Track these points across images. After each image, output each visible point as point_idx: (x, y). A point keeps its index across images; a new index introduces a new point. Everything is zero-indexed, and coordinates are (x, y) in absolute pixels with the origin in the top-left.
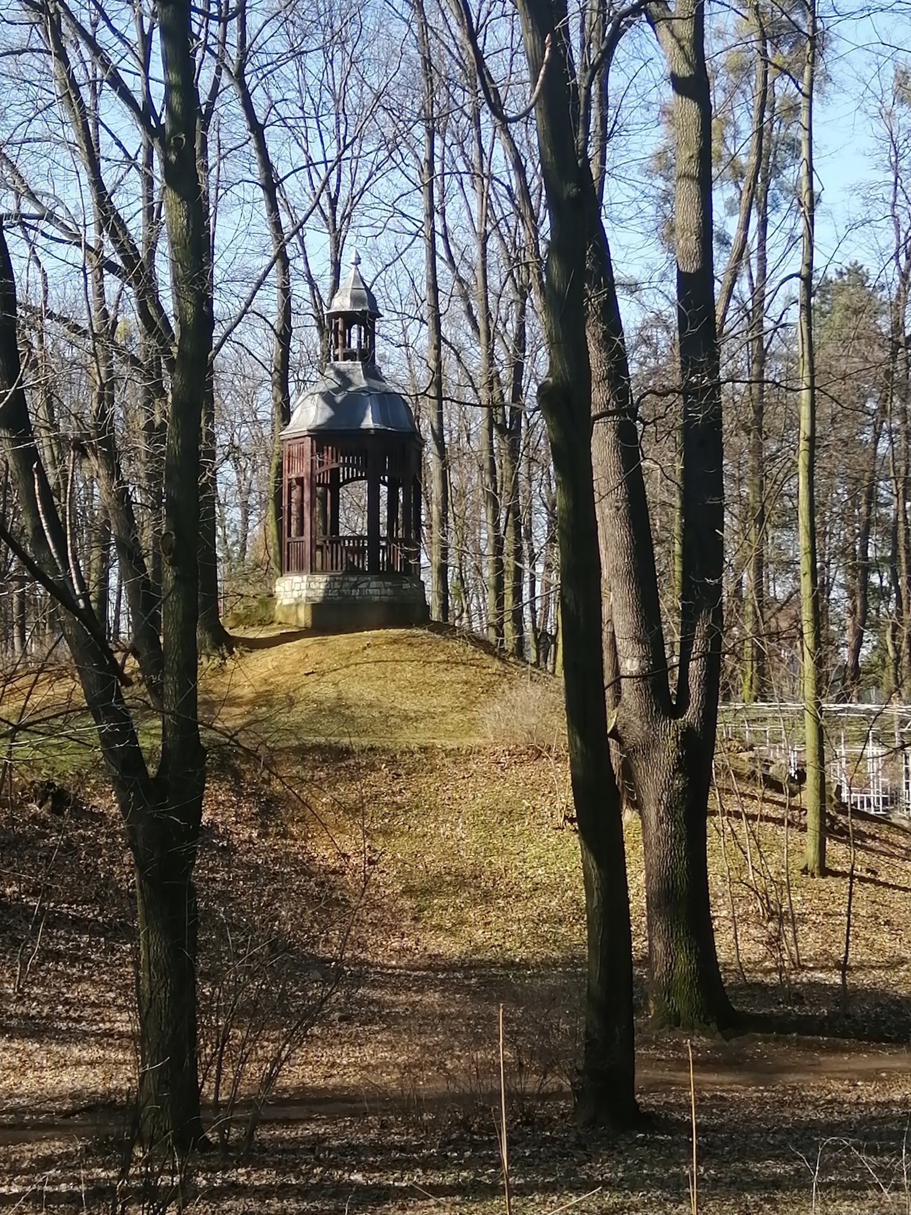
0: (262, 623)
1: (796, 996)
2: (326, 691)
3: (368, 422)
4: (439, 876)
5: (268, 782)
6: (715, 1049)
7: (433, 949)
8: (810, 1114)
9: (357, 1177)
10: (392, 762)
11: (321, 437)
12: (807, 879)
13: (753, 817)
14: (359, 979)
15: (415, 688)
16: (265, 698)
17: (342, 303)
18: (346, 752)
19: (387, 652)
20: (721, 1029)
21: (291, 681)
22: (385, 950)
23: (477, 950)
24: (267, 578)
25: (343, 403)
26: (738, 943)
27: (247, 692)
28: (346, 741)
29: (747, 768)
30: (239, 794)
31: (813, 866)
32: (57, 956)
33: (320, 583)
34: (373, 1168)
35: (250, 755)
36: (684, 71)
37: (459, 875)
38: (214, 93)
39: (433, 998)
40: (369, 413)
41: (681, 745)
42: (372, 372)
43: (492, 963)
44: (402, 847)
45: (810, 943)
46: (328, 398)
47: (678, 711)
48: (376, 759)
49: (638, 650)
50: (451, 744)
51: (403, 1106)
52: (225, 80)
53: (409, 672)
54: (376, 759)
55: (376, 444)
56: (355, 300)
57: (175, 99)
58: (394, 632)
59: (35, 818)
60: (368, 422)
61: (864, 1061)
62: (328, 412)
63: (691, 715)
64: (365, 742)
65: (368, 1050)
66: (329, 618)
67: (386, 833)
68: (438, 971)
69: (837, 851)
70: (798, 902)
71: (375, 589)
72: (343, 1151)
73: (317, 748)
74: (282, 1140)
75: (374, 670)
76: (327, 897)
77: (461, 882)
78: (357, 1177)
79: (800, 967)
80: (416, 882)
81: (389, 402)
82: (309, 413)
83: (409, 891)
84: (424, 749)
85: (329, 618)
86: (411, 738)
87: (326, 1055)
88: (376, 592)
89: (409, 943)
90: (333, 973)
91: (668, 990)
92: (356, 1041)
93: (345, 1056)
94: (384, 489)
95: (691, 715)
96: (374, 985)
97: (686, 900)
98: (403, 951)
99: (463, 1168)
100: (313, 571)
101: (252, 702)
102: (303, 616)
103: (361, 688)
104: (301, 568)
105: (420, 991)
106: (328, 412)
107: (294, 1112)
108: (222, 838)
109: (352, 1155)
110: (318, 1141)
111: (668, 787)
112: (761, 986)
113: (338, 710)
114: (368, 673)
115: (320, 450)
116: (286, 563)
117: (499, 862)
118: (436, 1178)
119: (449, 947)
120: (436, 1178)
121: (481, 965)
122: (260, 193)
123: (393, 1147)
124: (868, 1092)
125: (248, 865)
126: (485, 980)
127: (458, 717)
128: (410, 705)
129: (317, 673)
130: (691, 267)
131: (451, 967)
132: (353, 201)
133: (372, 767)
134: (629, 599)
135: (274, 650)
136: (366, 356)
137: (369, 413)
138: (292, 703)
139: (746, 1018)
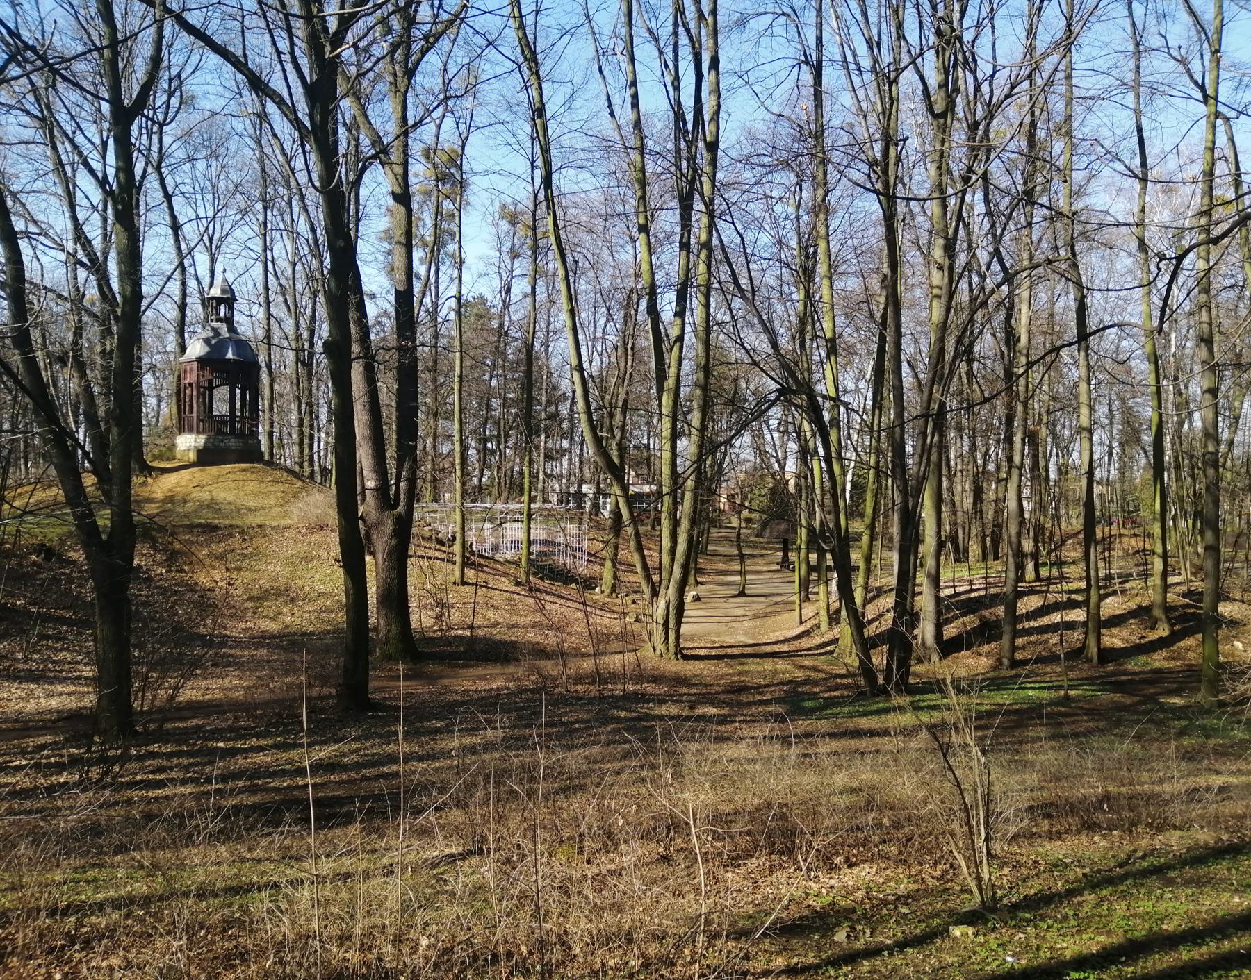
0: (168, 459)
1: (449, 641)
2: (205, 495)
3: (230, 355)
4: (267, 591)
5: (171, 543)
6: (409, 670)
7: (263, 627)
8: (455, 698)
9: (221, 744)
10: (242, 533)
11: (201, 360)
12: (455, 587)
13: (430, 558)
14: (223, 644)
15: (256, 494)
16: (170, 499)
17: (216, 292)
18: (216, 528)
19: (240, 476)
22: (235, 629)
23: (287, 627)
25: (216, 346)
26: (421, 619)
27: (159, 496)
29: (428, 535)
30: (155, 550)
31: (458, 581)
32: (48, 637)
33: (202, 439)
34: (229, 739)
35: (162, 529)
36: (398, 191)
37: (278, 589)
38: (144, 176)
42: (232, 329)
43: (295, 634)
44: (247, 576)
45: (456, 617)
46: (207, 341)
47: (395, 506)
50: (275, 523)
53: (252, 486)
55: (233, 366)
56: (223, 291)
57: (121, 176)
59: (34, 564)
60: (230, 355)
61: (480, 671)
62: (207, 349)
63: (401, 508)
64: (227, 522)
65: (227, 680)
66: (206, 457)
67: (239, 569)
68: (265, 639)
69: (470, 573)
70: (451, 597)
71: (232, 443)
72: (212, 732)
73: (200, 525)
74: (179, 728)
75: (232, 485)
76: (205, 603)
77: (279, 593)
78: (221, 744)
79: (450, 628)
80: (254, 594)
81: (241, 345)
82: (196, 348)
83: (251, 599)
84: (260, 526)
85: (206, 457)
87: (204, 684)
88: (232, 444)
89: (249, 625)
90: (207, 642)
91: (386, 643)
92: (220, 676)
93: (214, 684)
94: (238, 391)
95: (401, 508)
96: (231, 647)
97: (396, 598)
98: (247, 629)
100: (198, 432)
101: (164, 501)
102: (192, 456)
103: (224, 494)
104: (191, 431)
105: (256, 649)
106: (207, 349)
108: (145, 573)
109: (218, 734)
110: (199, 727)
112: (431, 639)
113: (212, 505)
114: (228, 487)
116: (183, 427)
117: (300, 583)
118: (263, 742)
119: (272, 626)
120: (263, 742)
121: (289, 634)
122: (170, 231)
123: (241, 728)
124: (481, 685)
126: (291, 643)
127: (278, 509)
128: (252, 503)
129: (200, 486)
130: (402, 288)
131: (273, 637)
132: (222, 239)
133: (231, 535)
135: (175, 474)
136: (229, 320)
138: (185, 502)
139: (422, 654)
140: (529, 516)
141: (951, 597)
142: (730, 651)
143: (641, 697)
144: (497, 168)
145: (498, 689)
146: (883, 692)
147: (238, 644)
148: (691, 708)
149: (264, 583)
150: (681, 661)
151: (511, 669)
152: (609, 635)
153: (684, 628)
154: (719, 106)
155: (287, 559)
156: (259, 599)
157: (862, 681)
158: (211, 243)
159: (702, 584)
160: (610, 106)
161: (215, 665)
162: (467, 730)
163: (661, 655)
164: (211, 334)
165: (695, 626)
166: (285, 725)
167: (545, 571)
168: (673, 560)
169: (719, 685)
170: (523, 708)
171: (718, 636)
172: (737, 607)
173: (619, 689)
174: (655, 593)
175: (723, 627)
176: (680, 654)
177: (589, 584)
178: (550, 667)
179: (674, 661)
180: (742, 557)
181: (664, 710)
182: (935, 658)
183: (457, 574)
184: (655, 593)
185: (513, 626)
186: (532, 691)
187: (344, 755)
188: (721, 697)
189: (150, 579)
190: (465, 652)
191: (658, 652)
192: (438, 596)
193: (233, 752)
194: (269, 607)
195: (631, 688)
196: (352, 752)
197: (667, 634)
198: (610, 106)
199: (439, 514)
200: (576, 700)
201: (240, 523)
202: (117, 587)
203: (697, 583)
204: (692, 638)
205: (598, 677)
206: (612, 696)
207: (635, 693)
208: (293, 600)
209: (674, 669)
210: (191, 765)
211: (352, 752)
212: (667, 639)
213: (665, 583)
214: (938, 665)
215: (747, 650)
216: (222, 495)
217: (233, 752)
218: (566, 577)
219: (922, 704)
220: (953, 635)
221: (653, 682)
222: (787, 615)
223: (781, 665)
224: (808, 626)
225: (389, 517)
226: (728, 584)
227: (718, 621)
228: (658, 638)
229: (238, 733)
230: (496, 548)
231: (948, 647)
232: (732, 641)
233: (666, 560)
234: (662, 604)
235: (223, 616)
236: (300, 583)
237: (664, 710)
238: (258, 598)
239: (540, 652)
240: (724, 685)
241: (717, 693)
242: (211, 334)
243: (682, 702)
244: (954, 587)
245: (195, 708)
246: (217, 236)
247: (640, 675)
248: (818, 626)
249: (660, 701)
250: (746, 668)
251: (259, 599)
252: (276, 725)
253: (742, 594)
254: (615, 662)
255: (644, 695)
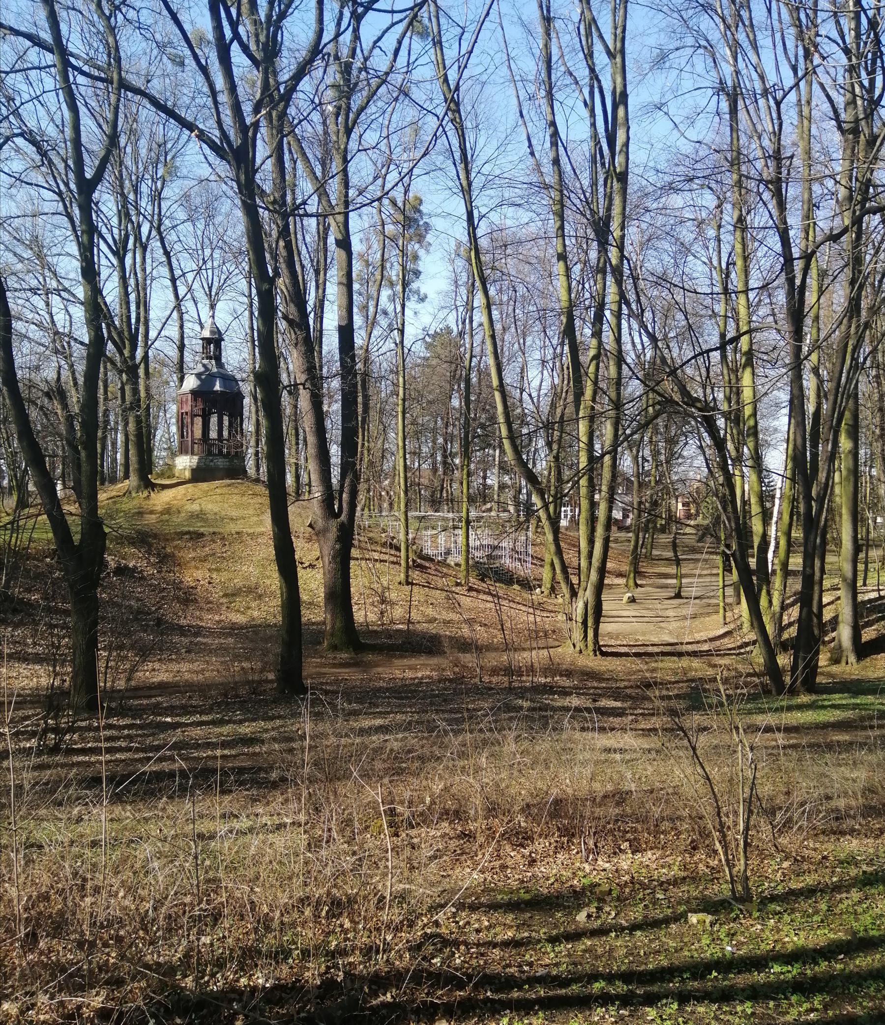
0: (169, 477)
1: (389, 634)
2: (195, 507)
3: (217, 387)
4: (240, 589)
5: (164, 548)
7: (234, 620)
8: (382, 684)
9: (169, 719)
10: (223, 539)
11: (194, 393)
13: (376, 560)
14: (196, 635)
15: (238, 506)
16: (167, 511)
17: (206, 334)
18: (202, 535)
19: (225, 490)
20: (354, 650)
21: (180, 503)
22: (209, 620)
23: (254, 619)
24: (173, 455)
25: (206, 378)
26: (364, 613)
27: (159, 508)
28: (202, 530)
29: (383, 540)
30: (149, 554)
31: (403, 581)
33: (195, 459)
34: (177, 715)
35: (155, 536)
36: (340, 237)
37: (249, 587)
38: (148, 238)
39: (231, 640)
40: (218, 383)
41: (339, 530)
42: (220, 364)
45: (398, 612)
46: (198, 375)
47: (338, 516)
48: (215, 538)
49: (321, 488)
50: (251, 531)
51: (190, 687)
52: (154, 233)
53: (236, 499)
54: (215, 538)
55: (216, 398)
56: (212, 332)
58: (228, 481)
60: (217, 387)
61: (413, 661)
62: (199, 383)
63: (343, 517)
64: (211, 530)
66: (199, 475)
67: (218, 570)
68: (233, 629)
69: (415, 575)
70: (393, 596)
71: (221, 462)
72: (166, 709)
73: (188, 533)
74: (141, 705)
75: (219, 498)
76: (187, 598)
78: (169, 719)
81: (229, 380)
82: (191, 383)
83: (226, 595)
84: (238, 533)
85: (199, 475)
86: (233, 528)
87: (175, 667)
88: (219, 464)
89: (223, 617)
90: (182, 631)
91: (332, 635)
92: (192, 661)
93: (184, 667)
94: (226, 418)
95: (343, 517)
96: (204, 636)
97: (339, 595)
98: (219, 622)
99: (218, 713)
100: (193, 454)
101: (162, 513)
102: (188, 475)
103: (210, 506)
104: (186, 453)
106: (199, 383)
107: (153, 692)
108: (139, 573)
109: (171, 710)
110: (159, 703)
111: (333, 548)
112: (375, 632)
113: (200, 516)
114: (217, 500)
115: (195, 400)
117: (268, 582)
118: (205, 718)
120: (205, 718)
121: (255, 626)
122: (169, 283)
124: (409, 674)
125: (151, 585)
126: (250, 633)
127: (255, 519)
128: (234, 513)
129: (192, 500)
130: (344, 323)
131: (242, 628)
132: (220, 288)
133: (214, 541)
134: (317, 468)
135: (174, 490)
136: (218, 358)
137: (218, 383)
138: (179, 512)
140: (468, 522)
141: (876, 600)
142: (650, 649)
143: (549, 689)
144: (439, 211)
145: (422, 678)
146: (793, 692)
147: (211, 633)
148: (595, 701)
149: (238, 582)
150: (599, 657)
151: (434, 661)
152: (537, 632)
153: (604, 628)
154: (628, 138)
155: (259, 561)
156: (233, 595)
157: (767, 680)
158: (210, 291)
159: (641, 586)
160: (530, 146)
161: (189, 651)
162: (380, 713)
163: (581, 652)
164: (202, 369)
165: (624, 626)
166: (228, 704)
167: (490, 573)
168: (590, 563)
169: (629, 680)
170: (437, 696)
171: (644, 634)
172: (671, 609)
173: (527, 681)
174: (574, 594)
175: (651, 627)
176: (599, 650)
177: (527, 585)
178: (468, 659)
179: (593, 657)
180: (678, 562)
181: (566, 702)
182: (852, 658)
183: (403, 576)
184: (574, 594)
185: (449, 622)
186: (450, 681)
187: (266, 731)
188: (628, 691)
189: (143, 578)
190: (404, 643)
191: (578, 649)
192: (380, 594)
193: (174, 726)
194: (240, 602)
195: (543, 680)
196: (273, 729)
197: (586, 632)
198: (530, 146)
199: (384, 519)
200: (486, 691)
201: (221, 530)
202: (90, 585)
203: (637, 585)
204: (610, 635)
205: (509, 671)
206: (521, 688)
207: (545, 685)
208: (260, 597)
209: (590, 664)
210: (137, 736)
211: (273, 729)
212: (586, 636)
213: (583, 584)
214: (855, 666)
215: (668, 649)
216: (210, 506)
217: (174, 726)
218: (507, 578)
219: (826, 703)
220: (874, 637)
221: (566, 676)
222: (715, 617)
223: (696, 663)
224: (732, 626)
225: (333, 525)
226: (666, 587)
227: (632, 619)
228: (577, 635)
229: (186, 710)
230: (448, 553)
231: (863, 650)
232: (655, 640)
233: (584, 564)
234: (580, 605)
235: (201, 609)
236: (268, 582)
237: (566, 702)
238: (232, 595)
239: (464, 645)
240: (636, 680)
241: (626, 687)
242: (202, 369)
243: (587, 694)
244: (879, 590)
245: (163, 688)
246: (216, 284)
247: (552, 669)
248: (740, 627)
249: (565, 692)
250: (660, 665)
251: (233, 595)
252: (219, 705)
253: (678, 596)
254: (523, 658)
255: (552, 687)
